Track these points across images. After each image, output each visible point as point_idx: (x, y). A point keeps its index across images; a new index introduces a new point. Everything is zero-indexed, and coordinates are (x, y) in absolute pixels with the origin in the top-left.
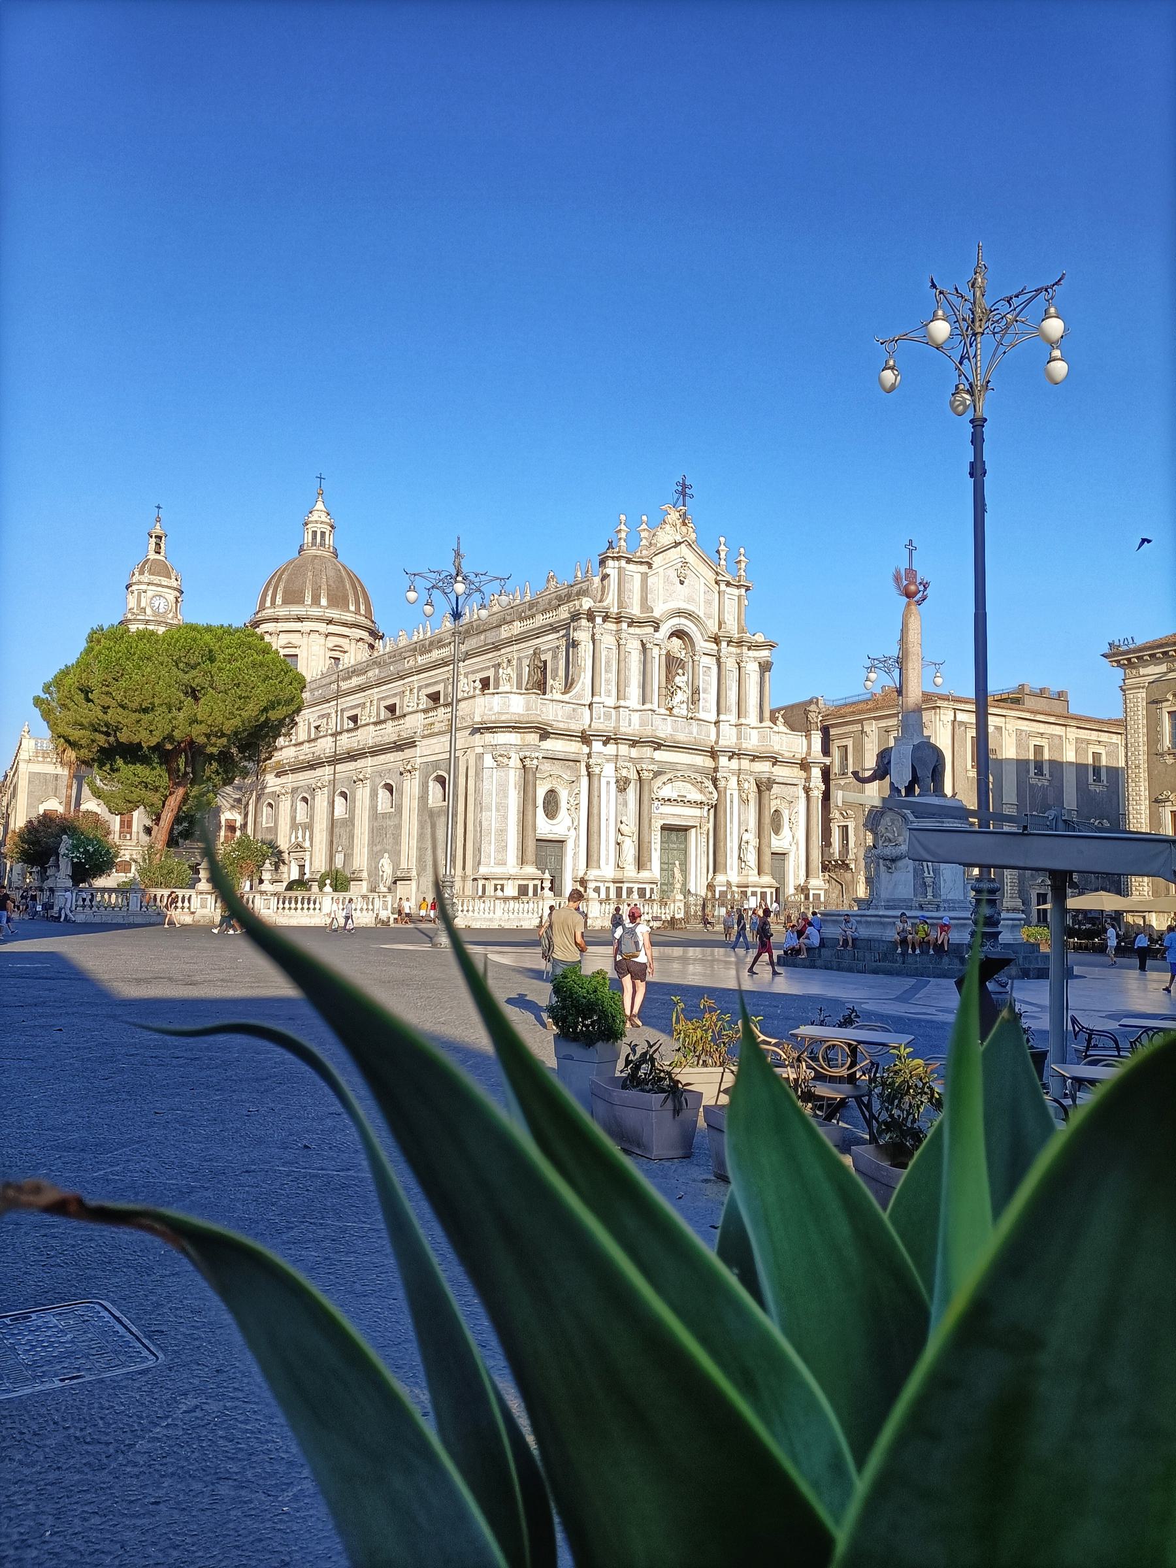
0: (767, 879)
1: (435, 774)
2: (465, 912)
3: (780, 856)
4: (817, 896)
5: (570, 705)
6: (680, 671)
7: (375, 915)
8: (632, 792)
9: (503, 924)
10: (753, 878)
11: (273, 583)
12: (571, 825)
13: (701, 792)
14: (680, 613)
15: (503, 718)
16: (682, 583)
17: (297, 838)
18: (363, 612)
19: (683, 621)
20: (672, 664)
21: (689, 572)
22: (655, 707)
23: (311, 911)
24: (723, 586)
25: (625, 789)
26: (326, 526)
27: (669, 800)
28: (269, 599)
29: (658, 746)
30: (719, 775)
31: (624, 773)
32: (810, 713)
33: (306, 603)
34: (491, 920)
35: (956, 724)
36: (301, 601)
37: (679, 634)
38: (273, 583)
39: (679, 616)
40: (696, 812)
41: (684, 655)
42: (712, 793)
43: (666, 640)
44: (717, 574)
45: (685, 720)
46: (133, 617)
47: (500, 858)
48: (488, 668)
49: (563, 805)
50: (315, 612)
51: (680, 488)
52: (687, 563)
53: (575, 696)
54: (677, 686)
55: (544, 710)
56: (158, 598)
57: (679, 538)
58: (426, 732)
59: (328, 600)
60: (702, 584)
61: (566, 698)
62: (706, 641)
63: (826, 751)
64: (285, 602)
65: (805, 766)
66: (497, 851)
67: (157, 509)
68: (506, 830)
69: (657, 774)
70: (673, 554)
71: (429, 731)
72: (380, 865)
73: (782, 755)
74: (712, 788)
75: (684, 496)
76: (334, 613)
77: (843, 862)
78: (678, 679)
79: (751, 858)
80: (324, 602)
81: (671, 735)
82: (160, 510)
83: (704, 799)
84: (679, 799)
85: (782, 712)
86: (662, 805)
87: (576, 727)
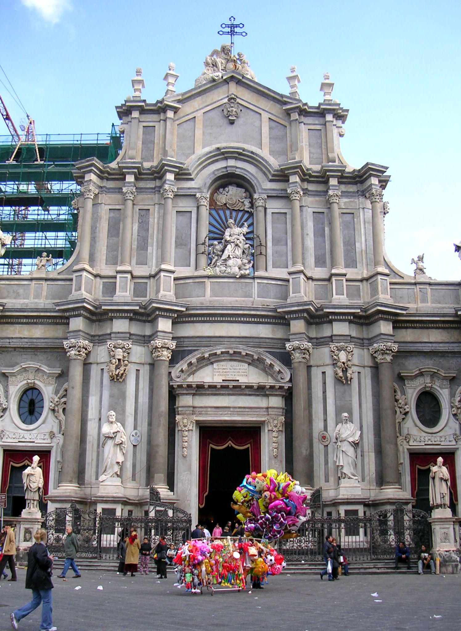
12: (56, 430)
24: (295, 116)
39: (226, 159)
44: (285, 103)
49: (47, 404)
51: (229, 30)
55: (21, 291)
62: (271, 181)
74: (278, 366)
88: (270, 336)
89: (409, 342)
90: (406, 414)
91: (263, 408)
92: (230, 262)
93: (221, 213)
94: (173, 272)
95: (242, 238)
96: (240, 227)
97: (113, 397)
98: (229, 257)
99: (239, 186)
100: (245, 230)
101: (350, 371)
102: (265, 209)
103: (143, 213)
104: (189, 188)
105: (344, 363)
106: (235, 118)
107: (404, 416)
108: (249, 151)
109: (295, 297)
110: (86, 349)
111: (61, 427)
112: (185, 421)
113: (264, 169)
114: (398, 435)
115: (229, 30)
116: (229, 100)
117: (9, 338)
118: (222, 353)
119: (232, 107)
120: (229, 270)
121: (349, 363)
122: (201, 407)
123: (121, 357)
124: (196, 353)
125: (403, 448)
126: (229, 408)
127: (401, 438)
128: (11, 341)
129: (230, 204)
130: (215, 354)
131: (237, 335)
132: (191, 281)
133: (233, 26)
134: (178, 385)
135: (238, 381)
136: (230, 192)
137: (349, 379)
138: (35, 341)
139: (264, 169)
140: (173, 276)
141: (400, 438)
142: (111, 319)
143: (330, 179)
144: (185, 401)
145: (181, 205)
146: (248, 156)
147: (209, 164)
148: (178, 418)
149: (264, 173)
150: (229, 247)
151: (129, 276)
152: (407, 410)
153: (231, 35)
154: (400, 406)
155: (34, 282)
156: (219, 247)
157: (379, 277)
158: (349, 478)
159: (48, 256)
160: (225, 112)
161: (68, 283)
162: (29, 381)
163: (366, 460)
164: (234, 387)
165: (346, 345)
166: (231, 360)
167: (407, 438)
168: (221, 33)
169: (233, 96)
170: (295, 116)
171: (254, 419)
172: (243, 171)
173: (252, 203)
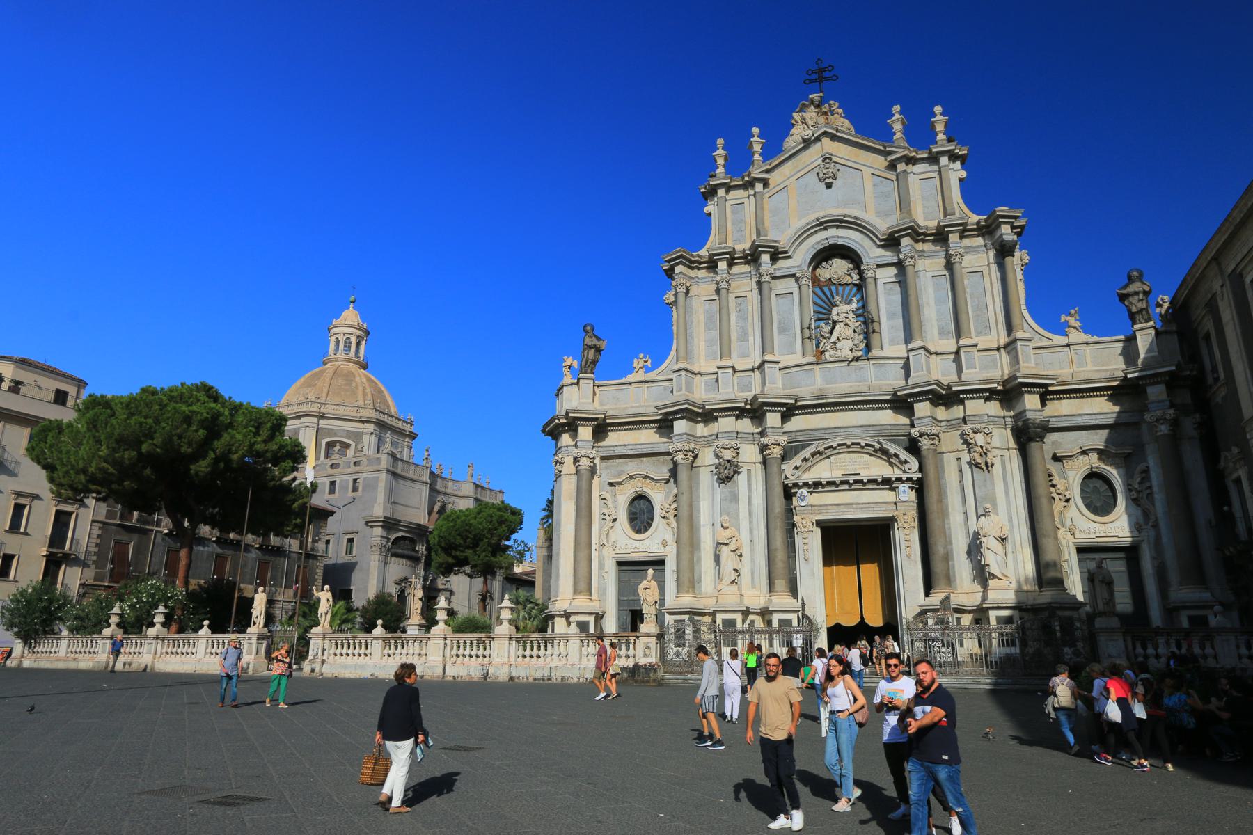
13: (891, 464)
14: (823, 225)
16: (829, 186)
19: (833, 232)
24: (901, 167)
31: (728, 455)
32: (1131, 299)
39: (825, 229)
42: (906, 462)
44: (890, 153)
45: (845, 364)
49: (658, 512)
57: (808, 133)
61: (652, 376)
70: (813, 156)
74: (904, 455)
81: (821, 390)
83: (897, 473)
86: (811, 493)
88: (893, 422)
89: (1065, 416)
90: (1067, 500)
91: (890, 502)
92: (839, 345)
93: (826, 289)
94: (778, 362)
95: (851, 315)
96: (848, 304)
97: (726, 500)
98: (838, 339)
99: (843, 257)
100: (854, 306)
101: (990, 455)
102: (875, 279)
103: (740, 300)
104: (788, 268)
105: (982, 447)
106: (831, 180)
107: (1065, 504)
108: (851, 217)
109: (918, 377)
110: (693, 452)
113: (870, 234)
114: (1059, 526)
115: (816, 76)
116: (823, 161)
117: (613, 446)
118: (839, 445)
119: (828, 168)
120: (838, 354)
121: (988, 447)
122: (821, 506)
123: (729, 458)
124: (810, 447)
125: (1067, 541)
126: (852, 504)
127: (1063, 530)
128: (616, 448)
129: (835, 279)
130: (831, 447)
132: (798, 369)
133: (820, 71)
134: (793, 484)
136: (834, 265)
137: (990, 465)
138: (640, 447)
139: (870, 234)
140: (778, 366)
141: (1063, 530)
142: (716, 419)
143: (950, 235)
144: (804, 499)
145: (780, 287)
147: (807, 237)
148: (796, 518)
149: (872, 239)
150: (837, 327)
151: (730, 370)
152: (1068, 497)
153: (819, 82)
154: (1058, 491)
157: (1019, 343)
158: (999, 579)
159: (644, 357)
160: (821, 175)
161: (668, 383)
162: (638, 489)
163: (1020, 557)
164: (856, 482)
165: (984, 426)
166: (849, 452)
167: (1072, 531)
168: (807, 82)
169: (827, 156)
170: (901, 167)
171: (881, 515)
172: (846, 240)
173: (861, 274)
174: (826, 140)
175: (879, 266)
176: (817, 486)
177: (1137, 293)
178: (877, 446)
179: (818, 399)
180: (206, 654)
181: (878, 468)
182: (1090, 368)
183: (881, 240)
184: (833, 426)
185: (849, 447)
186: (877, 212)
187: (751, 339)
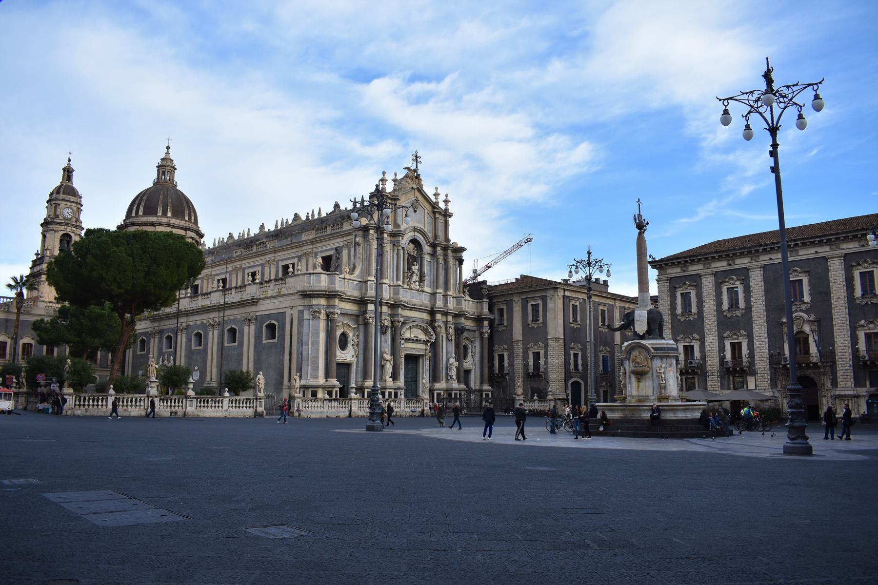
0: (463, 386)
1: (268, 322)
2: (307, 408)
3: (467, 372)
4: (487, 395)
5: (355, 282)
6: (415, 263)
7: (254, 410)
8: (389, 333)
9: (329, 415)
10: (455, 385)
11: (137, 202)
12: (354, 354)
13: (426, 334)
14: (415, 230)
15: (317, 289)
16: (415, 211)
17: (163, 361)
18: (193, 221)
19: (416, 234)
20: (411, 260)
21: (419, 206)
22: (402, 285)
23: (217, 408)
24: (437, 215)
25: (386, 333)
26: (171, 169)
27: (409, 339)
28: (134, 211)
29: (405, 307)
30: (436, 325)
33: (158, 214)
34: (321, 413)
35: (565, 297)
36: (155, 213)
37: (414, 241)
38: (137, 202)
39: (414, 231)
40: (423, 346)
41: (416, 253)
43: (407, 245)
46: (51, 220)
47: (315, 374)
48: (293, 258)
49: (350, 343)
50: (164, 220)
51: (414, 158)
52: (418, 200)
53: (357, 277)
54: (413, 272)
56: (67, 209)
57: (415, 186)
58: (262, 296)
59: (173, 213)
60: (426, 213)
61: (351, 277)
62: (428, 246)
63: (491, 310)
64: (146, 213)
65: (479, 320)
66: (313, 369)
67: (69, 154)
68: (318, 357)
69: (404, 323)
71: (264, 296)
72: (257, 379)
73: (469, 313)
74: (432, 333)
75: (417, 162)
76: (176, 222)
77: (502, 375)
78: (413, 267)
79: (454, 373)
80: (169, 214)
81: (410, 300)
82: (71, 155)
84: (415, 339)
85: (468, 288)
87: (356, 294)
111: (355, 353)
112: (403, 353)
130: (413, 325)
131: (418, 317)
135: (418, 337)
146: (422, 232)
149: (426, 242)
150: (415, 275)
155: (345, 280)
156: (410, 274)
174: (416, 191)
175: (428, 253)
176: (408, 340)
177: (485, 289)
178: (425, 327)
179: (412, 305)
180: (229, 407)
181: (422, 336)
182: (469, 310)
183: (430, 244)
184: (412, 316)
185: (419, 327)
186: (428, 230)
187: (389, 271)
